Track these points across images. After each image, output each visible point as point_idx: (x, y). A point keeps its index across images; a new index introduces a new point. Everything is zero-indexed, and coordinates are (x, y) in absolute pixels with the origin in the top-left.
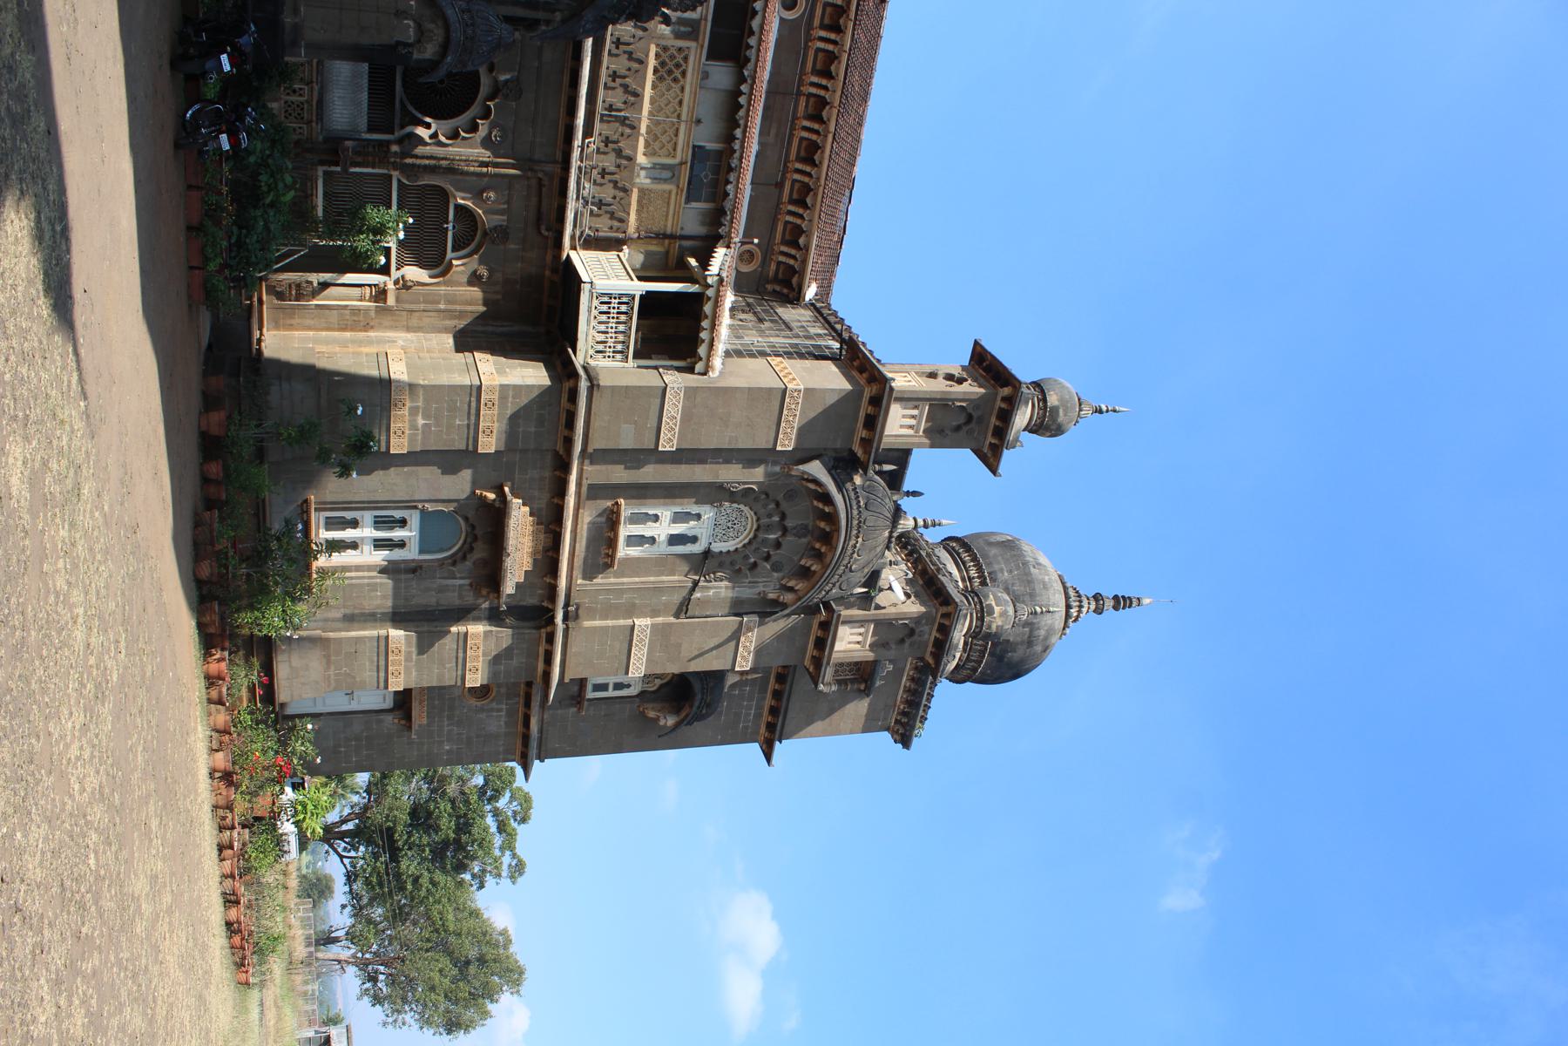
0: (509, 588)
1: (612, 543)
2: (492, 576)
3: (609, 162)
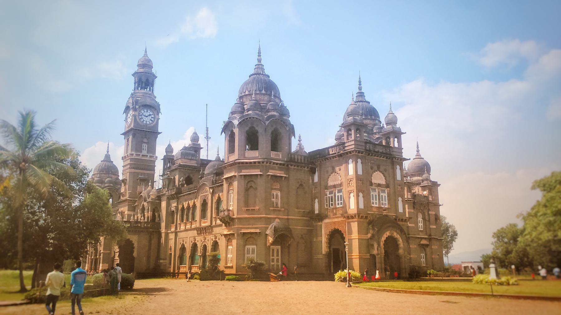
2: (427, 246)
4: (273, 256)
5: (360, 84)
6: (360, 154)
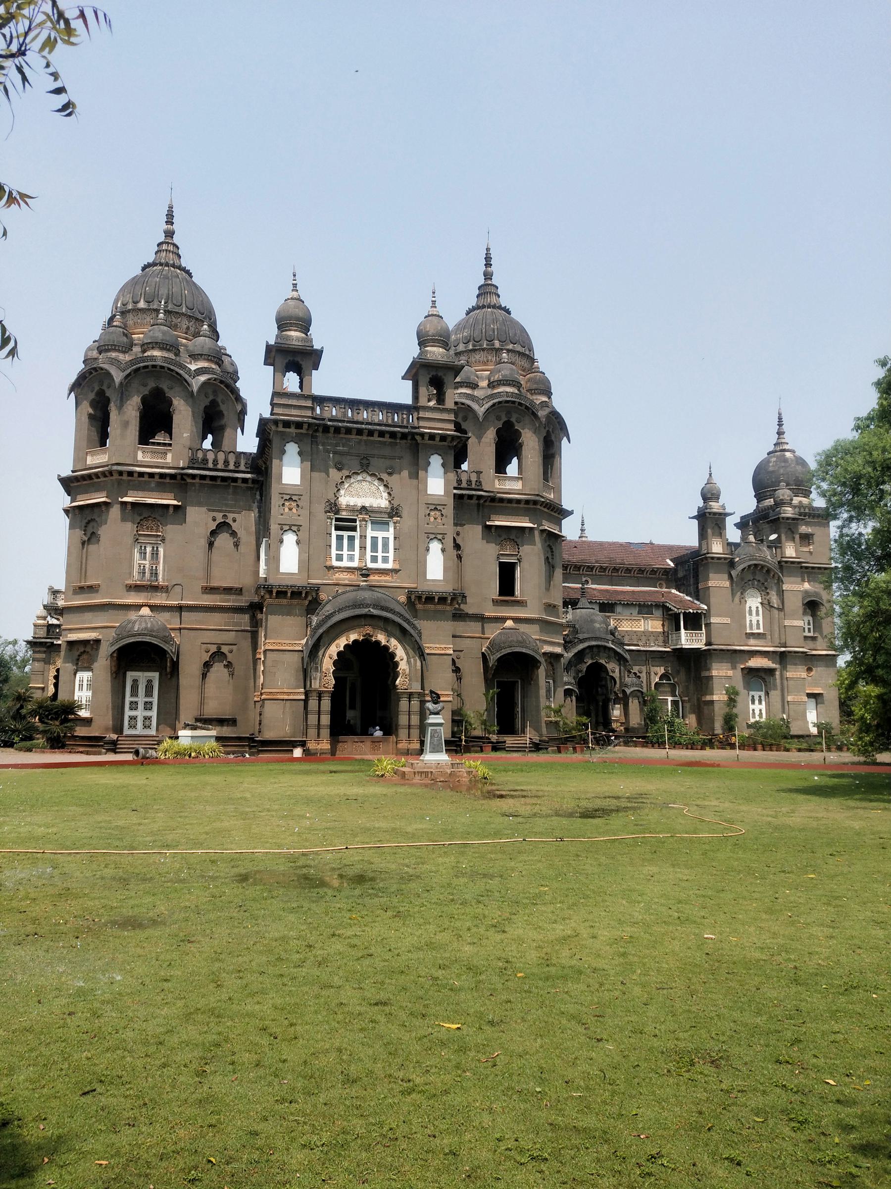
0: (773, 666)
1: (759, 634)
2: (771, 671)
3: (644, 638)
4: (135, 693)
5: (488, 264)
6: (292, 430)
